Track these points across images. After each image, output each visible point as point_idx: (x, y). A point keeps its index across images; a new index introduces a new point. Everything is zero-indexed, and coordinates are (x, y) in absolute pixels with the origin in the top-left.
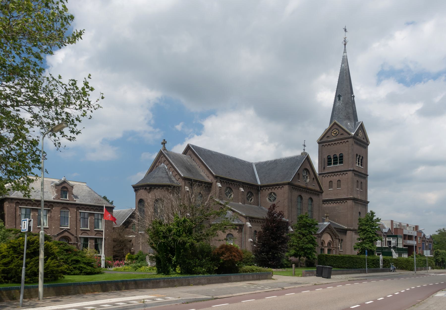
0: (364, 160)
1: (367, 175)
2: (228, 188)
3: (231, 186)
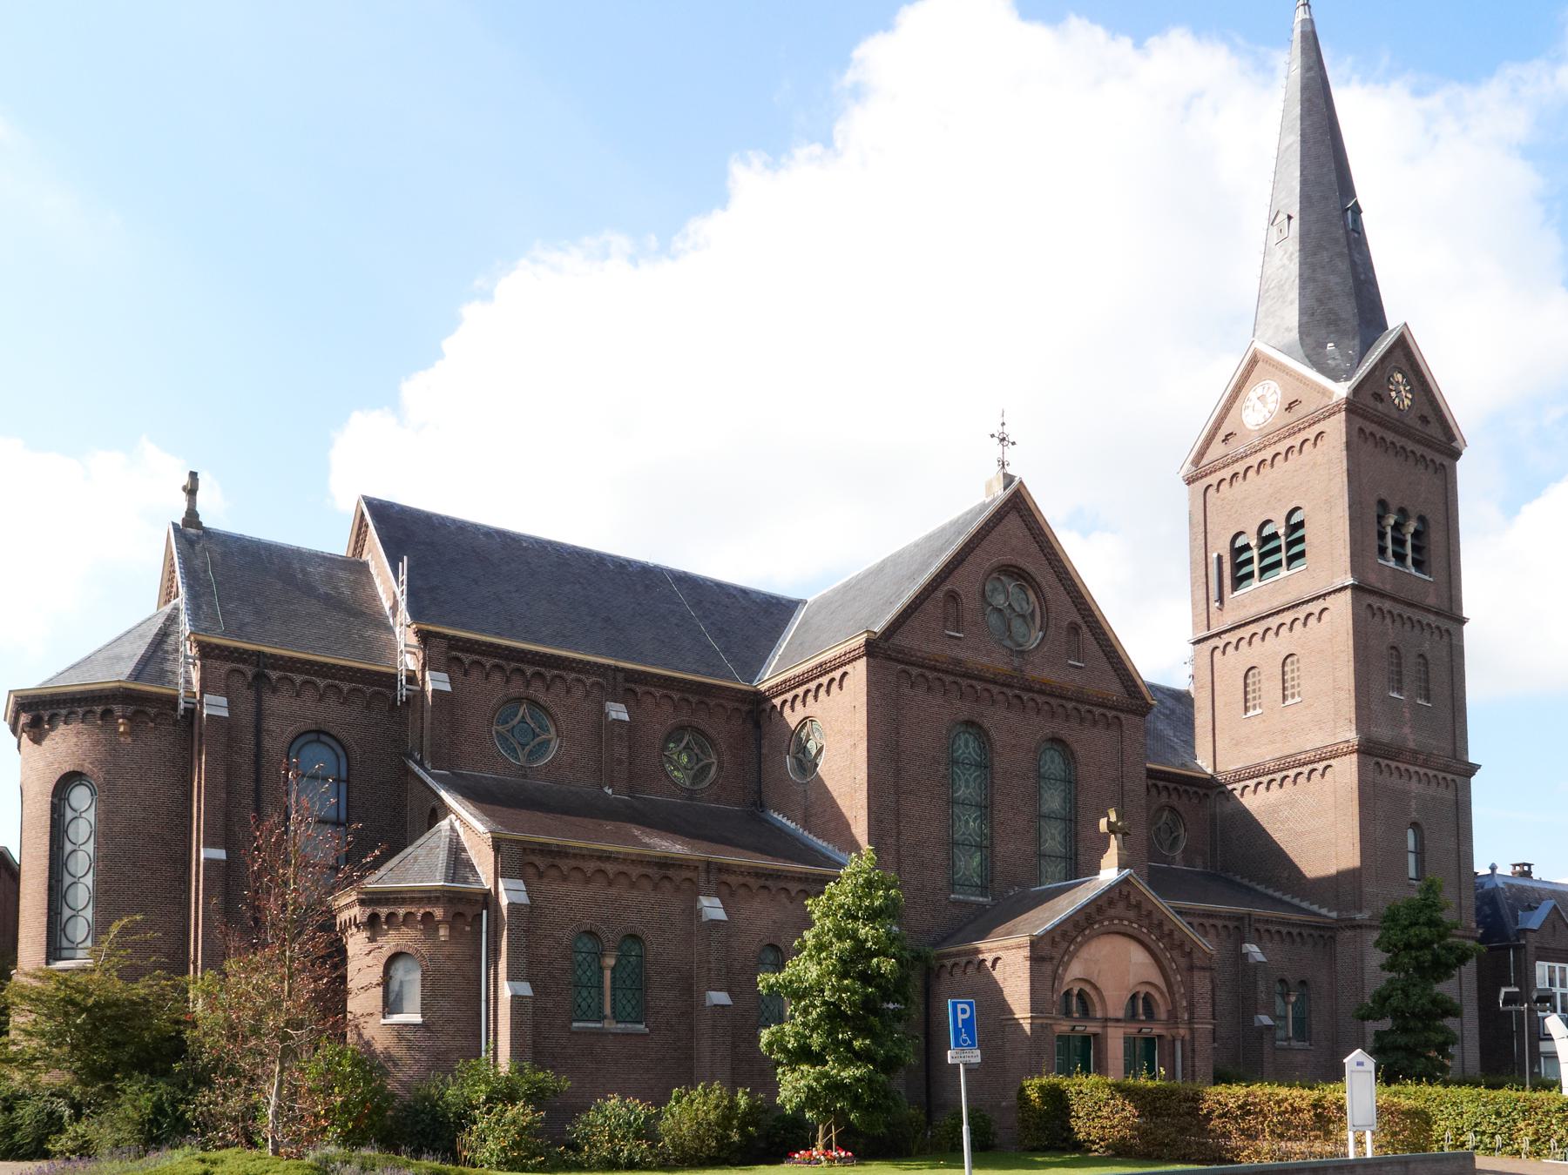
0: (1435, 537)
1: (1462, 621)
2: (519, 700)
3: (537, 691)
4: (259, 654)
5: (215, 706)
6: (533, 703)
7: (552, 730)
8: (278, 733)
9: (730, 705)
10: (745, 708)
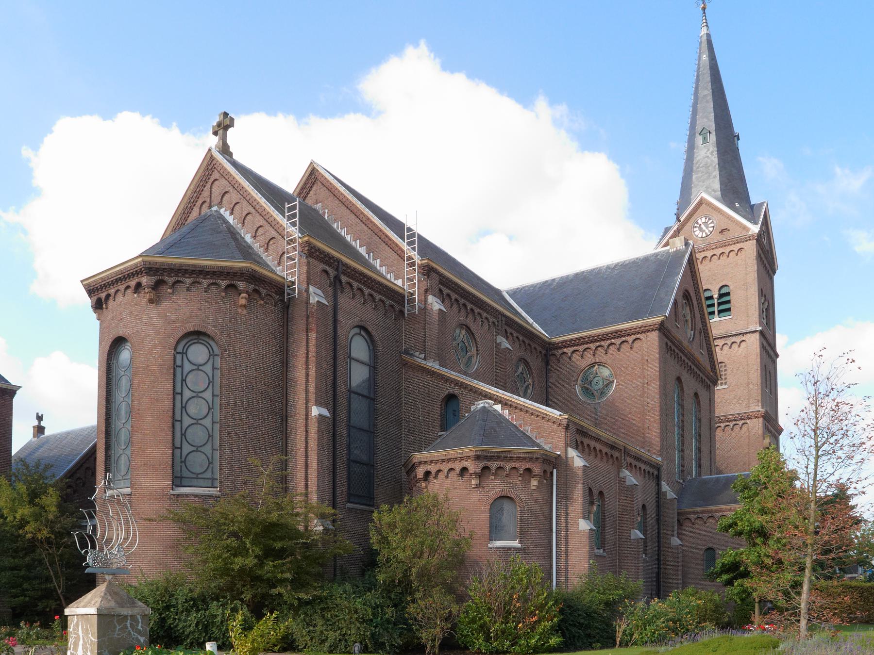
3: (470, 321)
4: (339, 261)
5: (316, 296)
6: (468, 329)
7: (474, 350)
8: (346, 323)
9: (539, 349)
10: (544, 352)
